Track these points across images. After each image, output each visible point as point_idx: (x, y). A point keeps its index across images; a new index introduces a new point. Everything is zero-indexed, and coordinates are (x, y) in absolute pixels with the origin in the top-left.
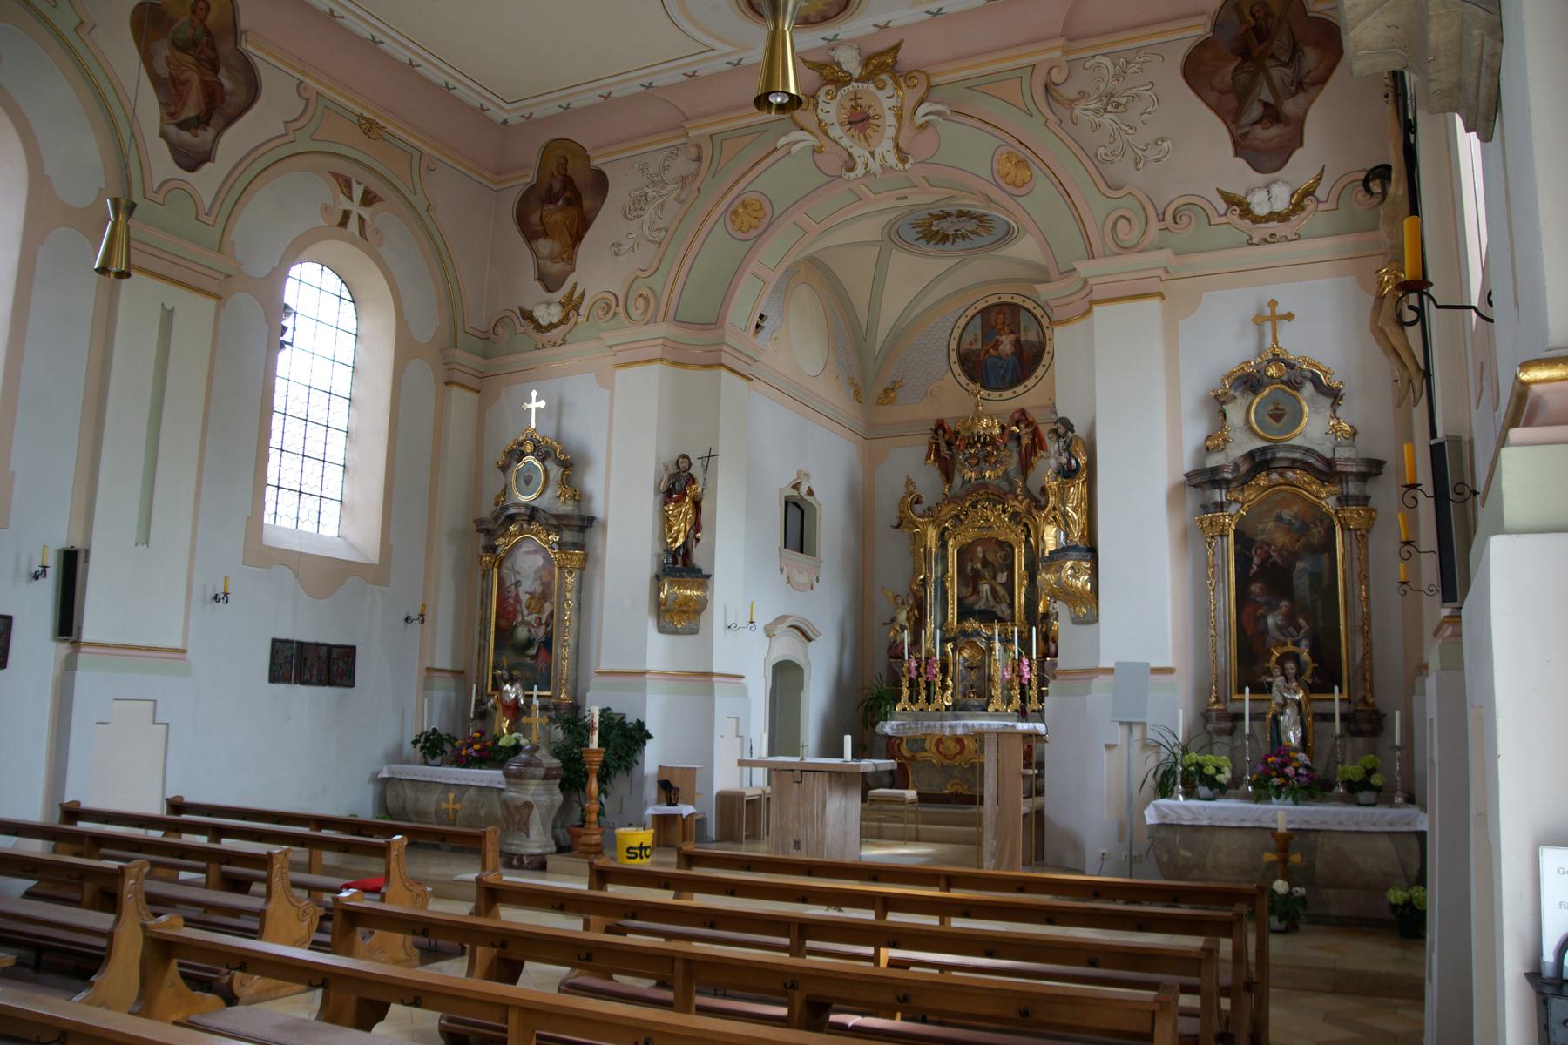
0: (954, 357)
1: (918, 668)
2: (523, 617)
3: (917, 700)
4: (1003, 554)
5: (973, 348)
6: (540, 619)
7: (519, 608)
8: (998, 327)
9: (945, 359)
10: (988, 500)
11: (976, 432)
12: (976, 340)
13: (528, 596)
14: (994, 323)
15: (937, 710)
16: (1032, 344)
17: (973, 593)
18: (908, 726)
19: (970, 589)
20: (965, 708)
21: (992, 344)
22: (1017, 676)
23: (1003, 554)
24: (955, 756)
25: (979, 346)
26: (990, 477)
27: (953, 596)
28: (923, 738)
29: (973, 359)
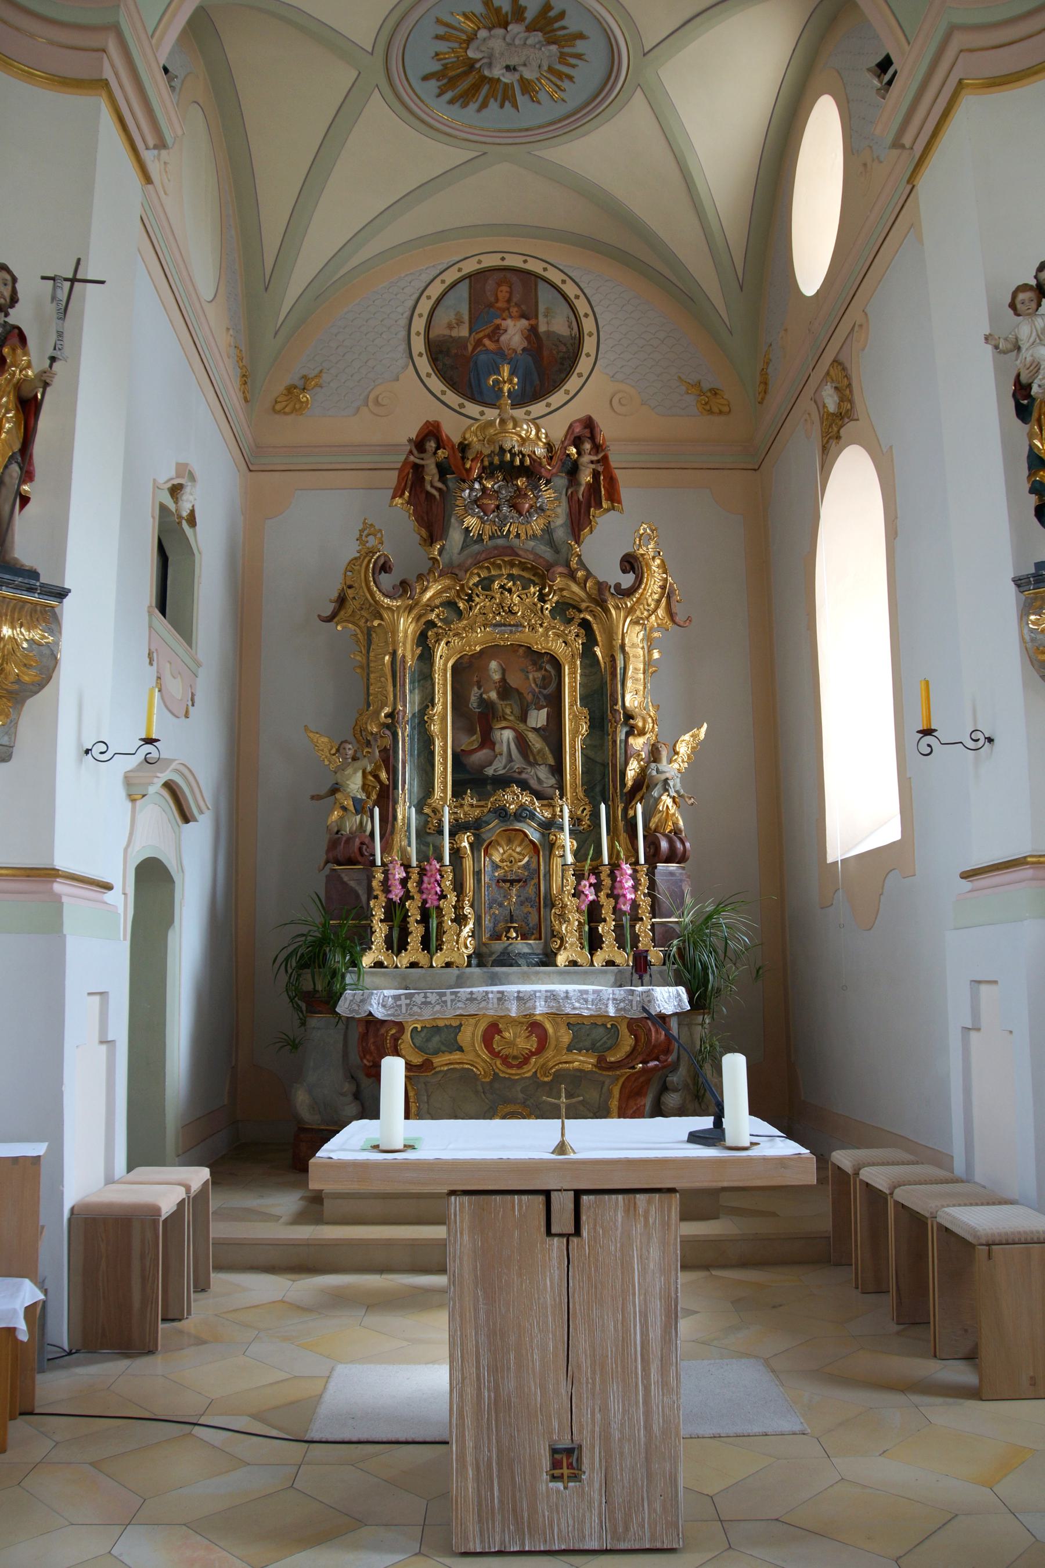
0: (419, 345)
1: (404, 882)
3: (403, 946)
4: (539, 675)
5: (454, 333)
8: (500, 305)
9: (403, 346)
10: (511, 577)
11: (507, 446)
12: (460, 322)
14: (492, 299)
15: (448, 965)
16: (559, 339)
17: (482, 746)
18: (419, 999)
19: (476, 738)
20: (506, 960)
21: (487, 332)
22: (608, 896)
23: (539, 675)
24: (526, 1060)
25: (464, 332)
26: (518, 536)
27: (445, 751)
28: (455, 1023)
29: (454, 351)
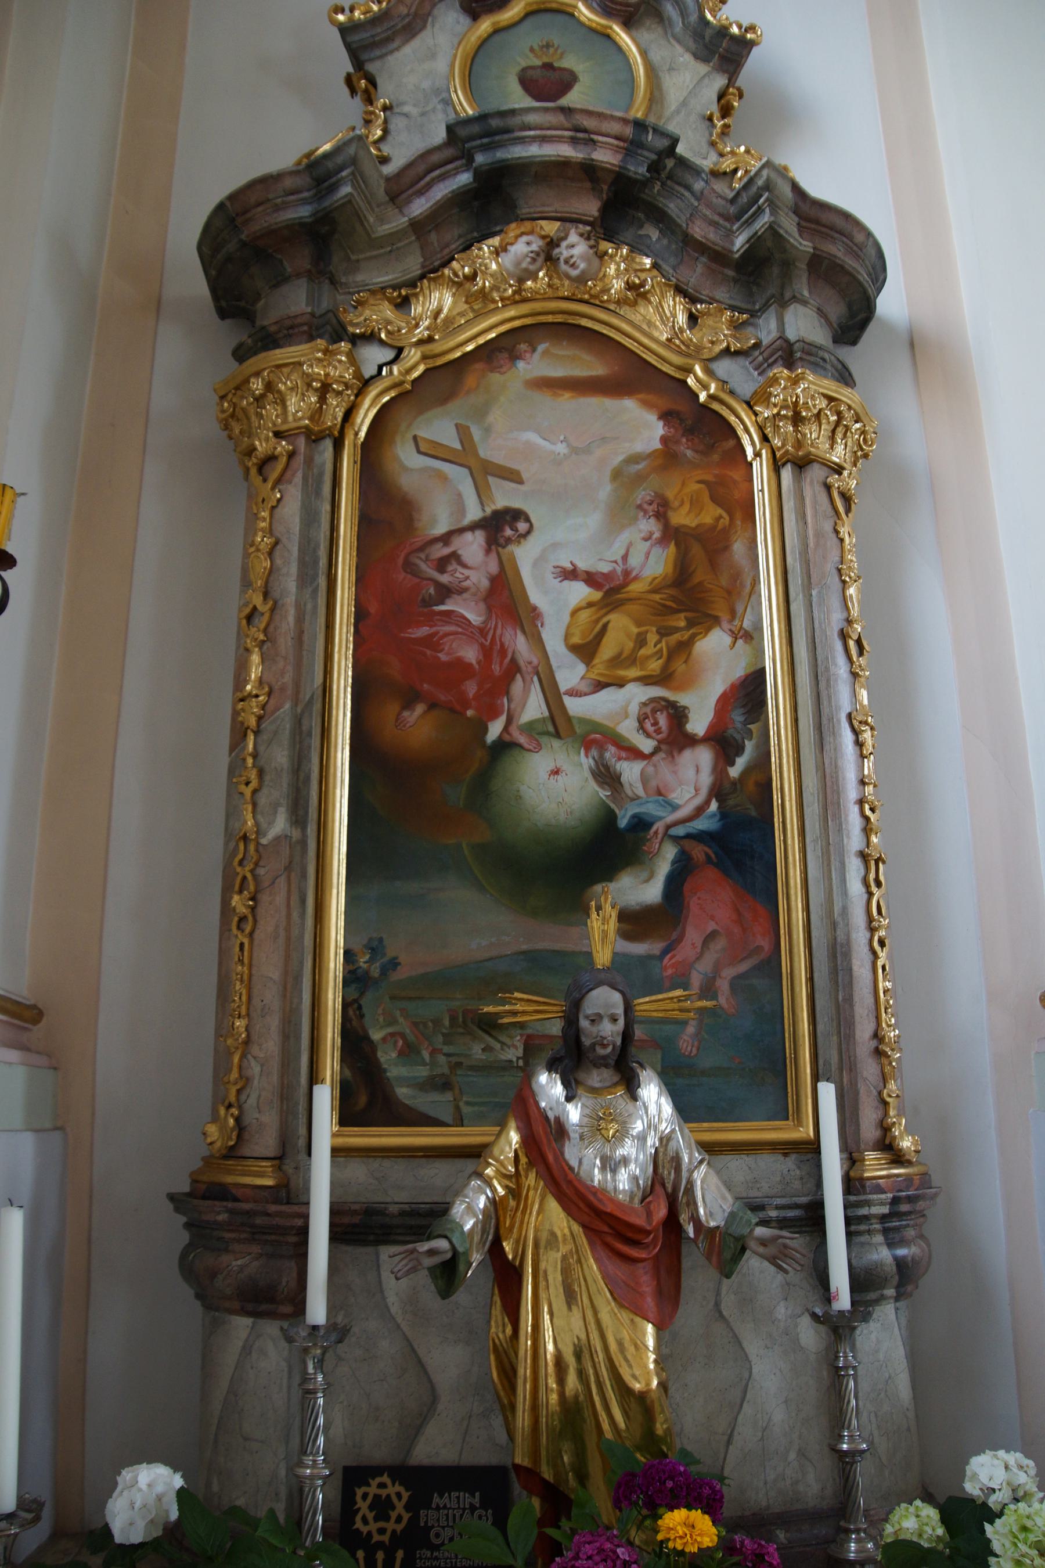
2: (552, 695)
6: (678, 715)
7: (520, 645)
13: (579, 592)
